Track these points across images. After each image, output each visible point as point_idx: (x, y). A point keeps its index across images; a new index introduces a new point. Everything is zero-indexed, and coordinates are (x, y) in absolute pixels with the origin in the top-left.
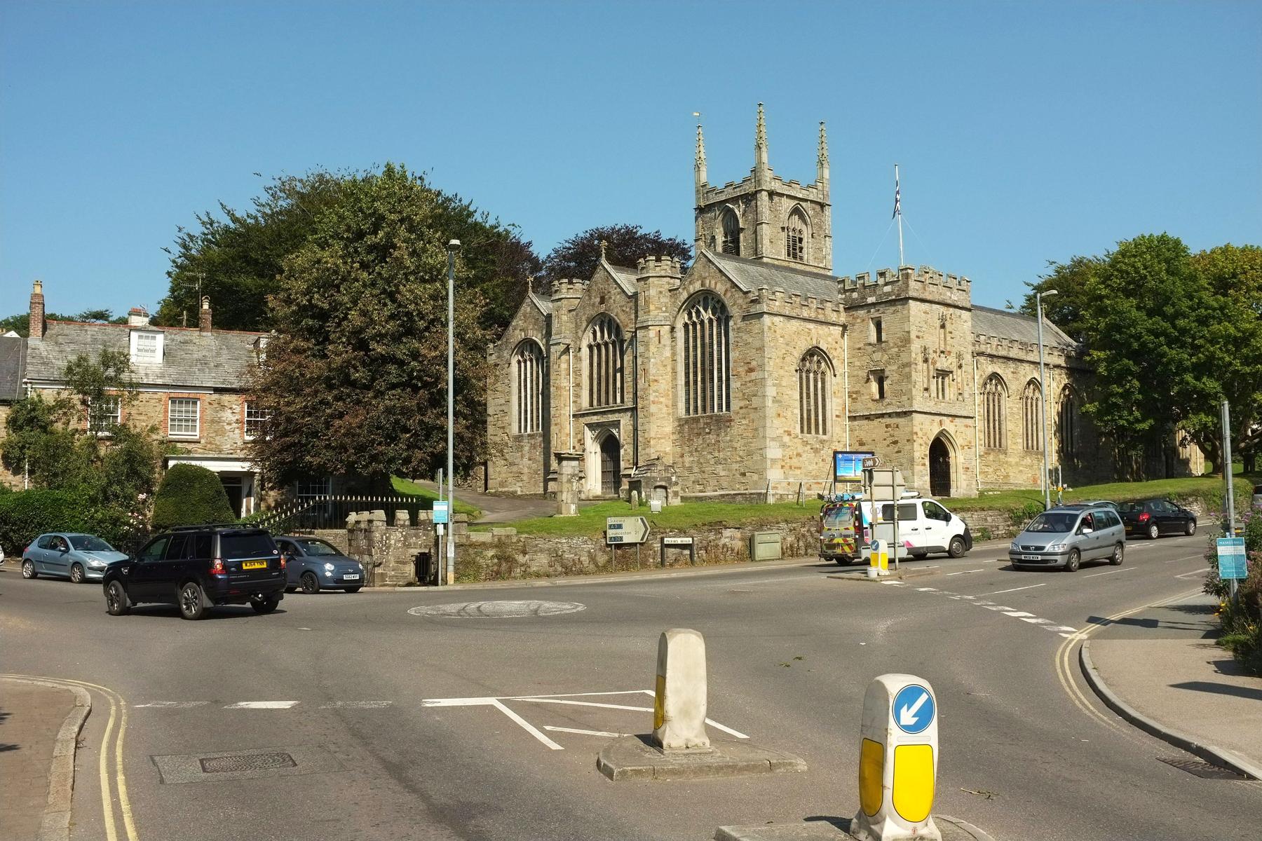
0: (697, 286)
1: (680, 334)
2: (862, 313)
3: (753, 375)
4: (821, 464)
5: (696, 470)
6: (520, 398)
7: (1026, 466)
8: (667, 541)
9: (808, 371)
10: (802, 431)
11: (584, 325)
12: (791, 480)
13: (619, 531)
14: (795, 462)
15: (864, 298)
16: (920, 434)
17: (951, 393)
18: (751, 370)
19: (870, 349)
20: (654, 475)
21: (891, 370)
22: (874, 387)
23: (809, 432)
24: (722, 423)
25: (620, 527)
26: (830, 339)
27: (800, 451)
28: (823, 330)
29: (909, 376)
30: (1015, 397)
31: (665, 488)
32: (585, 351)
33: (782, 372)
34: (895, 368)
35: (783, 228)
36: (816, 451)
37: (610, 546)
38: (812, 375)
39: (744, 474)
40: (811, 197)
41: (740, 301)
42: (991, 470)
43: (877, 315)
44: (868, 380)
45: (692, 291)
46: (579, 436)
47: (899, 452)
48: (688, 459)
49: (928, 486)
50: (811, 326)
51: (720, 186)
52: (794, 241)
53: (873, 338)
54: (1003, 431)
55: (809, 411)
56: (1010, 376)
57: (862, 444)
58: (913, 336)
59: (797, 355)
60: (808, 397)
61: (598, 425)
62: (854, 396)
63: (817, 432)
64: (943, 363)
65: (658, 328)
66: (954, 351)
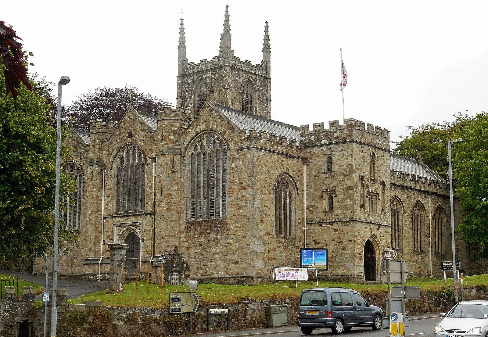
0: (203, 127)
1: (188, 161)
2: (317, 150)
3: (244, 192)
4: (289, 257)
5: (198, 259)
7: (415, 261)
8: (212, 311)
9: (281, 191)
10: (277, 233)
11: (115, 152)
13: (178, 303)
15: (319, 140)
16: (358, 237)
18: (243, 188)
19: (323, 176)
21: (339, 191)
22: (325, 203)
25: (178, 300)
27: (275, 247)
28: (291, 162)
29: (351, 196)
30: (408, 213)
31: (179, 272)
32: (114, 172)
33: (264, 190)
35: (240, 93)
36: (286, 247)
37: (172, 314)
38: (283, 193)
39: (236, 263)
40: (259, 73)
41: (236, 139)
43: (328, 152)
44: (322, 197)
45: (198, 131)
46: (108, 234)
47: (342, 249)
48: (192, 251)
49: (363, 274)
50: (283, 158)
51: (197, 62)
52: (247, 102)
54: (401, 237)
55: (281, 218)
56: (405, 198)
57: (316, 243)
58: (355, 168)
59: (274, 177)
60: (281, 209)
64: (373, 188)
65: (172, 157)
66: (379, 179)
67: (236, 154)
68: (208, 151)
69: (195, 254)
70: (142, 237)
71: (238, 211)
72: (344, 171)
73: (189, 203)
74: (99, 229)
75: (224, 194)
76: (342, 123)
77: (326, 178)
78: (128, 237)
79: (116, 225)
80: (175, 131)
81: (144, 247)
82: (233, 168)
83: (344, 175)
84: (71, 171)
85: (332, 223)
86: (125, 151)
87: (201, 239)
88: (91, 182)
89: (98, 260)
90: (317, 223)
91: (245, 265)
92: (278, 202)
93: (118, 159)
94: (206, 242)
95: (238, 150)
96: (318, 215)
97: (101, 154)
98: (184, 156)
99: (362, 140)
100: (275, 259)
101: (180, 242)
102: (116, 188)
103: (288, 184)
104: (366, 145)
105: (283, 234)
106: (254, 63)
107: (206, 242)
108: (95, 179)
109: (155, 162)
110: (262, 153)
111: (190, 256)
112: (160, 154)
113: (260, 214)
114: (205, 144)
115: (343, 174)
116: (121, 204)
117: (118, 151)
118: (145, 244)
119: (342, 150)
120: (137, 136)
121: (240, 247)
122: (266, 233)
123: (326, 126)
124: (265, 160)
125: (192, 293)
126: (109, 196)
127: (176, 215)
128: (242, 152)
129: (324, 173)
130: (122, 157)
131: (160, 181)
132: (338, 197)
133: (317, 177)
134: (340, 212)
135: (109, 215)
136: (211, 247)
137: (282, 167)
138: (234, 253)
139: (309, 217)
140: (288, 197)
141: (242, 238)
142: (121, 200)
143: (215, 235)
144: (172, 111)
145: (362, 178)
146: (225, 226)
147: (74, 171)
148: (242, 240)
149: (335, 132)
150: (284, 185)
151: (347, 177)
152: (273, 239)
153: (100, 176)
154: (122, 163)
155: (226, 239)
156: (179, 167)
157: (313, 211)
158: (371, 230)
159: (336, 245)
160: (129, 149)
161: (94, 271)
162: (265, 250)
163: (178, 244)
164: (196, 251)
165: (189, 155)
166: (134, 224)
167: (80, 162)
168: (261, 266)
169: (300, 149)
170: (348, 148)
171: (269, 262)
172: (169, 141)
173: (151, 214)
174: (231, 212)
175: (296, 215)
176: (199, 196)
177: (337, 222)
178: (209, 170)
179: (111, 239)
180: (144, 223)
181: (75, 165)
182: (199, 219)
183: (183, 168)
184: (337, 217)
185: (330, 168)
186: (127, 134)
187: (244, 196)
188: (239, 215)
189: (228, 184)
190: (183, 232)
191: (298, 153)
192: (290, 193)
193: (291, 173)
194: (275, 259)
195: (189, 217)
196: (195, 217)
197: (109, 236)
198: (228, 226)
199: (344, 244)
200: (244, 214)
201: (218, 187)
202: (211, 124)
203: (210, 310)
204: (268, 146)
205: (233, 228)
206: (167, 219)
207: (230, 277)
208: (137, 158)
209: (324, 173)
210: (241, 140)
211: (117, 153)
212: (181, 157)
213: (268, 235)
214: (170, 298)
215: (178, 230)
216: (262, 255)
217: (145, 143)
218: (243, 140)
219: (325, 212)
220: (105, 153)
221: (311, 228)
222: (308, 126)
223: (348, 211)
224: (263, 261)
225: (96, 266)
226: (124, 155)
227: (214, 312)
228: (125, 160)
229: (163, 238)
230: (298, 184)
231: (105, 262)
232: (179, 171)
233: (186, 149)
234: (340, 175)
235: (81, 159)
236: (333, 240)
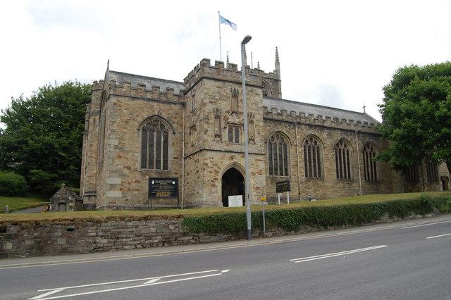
7: (340, 188)
16: (210, 165)
17: (244, 138)
28: (162, 106)
31: (65, 204)
42: (310, 190)
50: (155, 104)
54: (322, 168)
55: (151, 155)
59: (140, 119)
63: (158, 167)
64: (233, 119)
99: (221, 77)
104: (224, 81)
106: (267, 71)
113: (118, 150)
158: (232, 157)
193: (164, 115)
204: (133, 93)
213: (129, 168)
215: (95, 171)
224: (121, 192)
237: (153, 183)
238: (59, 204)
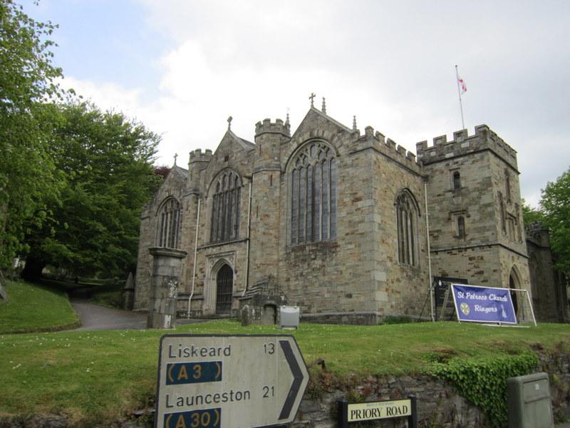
3: (360, 204)
5: (300, 292)
6: (161, 240)
9: (401, 209)
11: (211, 179)
12: (394, 303)
14: (395, 286)
15: (442, 155)
16: (503, 265)
18: (358, 199)
19: (450, 195)
20: (266, 293)
21: (474, 212)
22: (454, 227)
23: (404, 262)
24: (328, 248)
25: (211, 372)
26: (416, 186)
32: (210, 199)
33: (384, 203)
34: (477, 207)
36: (410, 278)
38: (403, 212)
39: (350, 296)
41: (346, 142)
43: (455, 166)
44: (449, 219)
45: (301, 141)
46: (201, 266)
48: (293, 283)
50: (403, 171)
53: (451, 186)
55: (403, 243)
58: (493, 180)
59: (394, 190)
61: (217, 256)
62: (435, 235)
63: (409, 263)
65: (270, 173)
67: (348, 161)
68: (312, 164)
69: (295, 286)
70: (236, 267)
71: (352, 229)
72: (479, 186)
73: (289, 226)
74: (191, 262)
75: (333, 210)
76: (471, 133)
77: (454, 197)
78: (220, 271)
79: (209, 256)
80: (274, 145)
81: (239, 281)
82: (344, 177)
83: (478, 191)
84: (172, 206)
85: (466, 249)
86: (222, 177)
87: (304, 268)
88: (187, 212)
89: (189, 295)
90: (444, 251)
91: (362, 299)
92: (400, 223)
93: (214, 186)
94: (310, 270)
95: (351, 153)
96: (446, 241)
97: (198, 183)
98: (284, 173)
100: (399, 293)
101: (278, 272)
102: (210, 216)
103: (408, 204)
105: (406, 261)
107: (310, 270)
108: (190, 208)
109: (252, 182)
110: (380, 157)
111: (289, 289)
112: (257, 171)
113: (381, 232)
114: (309, 155)
115: (476, 189)
116: (215, 234)
117: (215, 177)
118: (238, 276)
119: (473, 162)
120: (233, 158)
121: (355, 275)
122: (388, 257)
123: (450, 139)
124: (385, 167)
125: (278, 339)
126: (203, 226)
127: (274, 240)
128: (356, 156)
129: (450, 191)
130: (219, 184)
131: (256, 201)
132: (472, 218)
133: (441, 197)
134: (477, 235)
135: (203, 245)
136: (316, 277)
137: (402, 181)
138: (347, 284)
139: (433, 245)
140: (409, 218)
141: (357, 263)
142: (215, 229)
143: (320, 262)
144: (272, 125)
145: (500, 195)
146: (334, 250)
147: (175, 205)
148: (358, 266)
149: (461, 143)
150: (405, 200)
151: (483, 192)
152: (396, 266)
153: (195, 205)
154: (217, 191)
155: (336, 265)
156: (278, 185)
157: (438, 236)
159: (473, 276)
160: (226, 173)
161: (184, 308)
162: (388, 280)
163: (275, 274)
164: (297, 283)
165: (291, 171)
166: (227, 254)
167: (180, 196)
168: (384, 300)
169: (420, 166)
170: (482, 158)
171: (393, 296)
172: (267, 156)
173: (245, 241)
174: (341, 230)
175: (419, 241)
176: (300, 216)
177: (472, 248)
178: (313, 185)
179: (202, 272)
180: (238, 252)
181: (176, 200)
182: (302, 244)
183: (283, 186)
184: (473, 242)
185: (457, 186)
186: (223, 159)
187: (359, 209)
188: (352, 234)
189: (337, 197)
190: (282, 260)
191: (417, 169)
192: (411, 215)
194: (399, 293)
195: (289, 242)
196: (297, 241)
197: (201, 269)
198: (338, 249)
199: (486, 275)
200: (360, 232)
201: (324, 203)
202: (316, 132)
203: (351, 407)
205: (345, 251)
206: (262, 244)
207: (341, 316)
208: (233, 182)
209: (450, 191)
210: (354, 143)
211: (213, 180)
212: (281, 174)
213: (391, 261)
214: (166, 361)
215: (275, 257)
216: (385, 286)
217: (242, 164)
218: (357, 141)
219: (455, 237)
220: (202, 182)
221: (437, 257)
222: (426, 142)
223: (488, 234)
224: (386, 294)
225: (186, 302)
226: (220, 182)
227: (365, 413)
228: (221, 186)
229: (259, 267)
230: (419, 204)
231: (196, 297)
232: (278, 190)
233: (287, 163)
234: (474, 191)
235: (181, 193)
236: (469, 271)
237: (440, 284)
238: (266, 306)
